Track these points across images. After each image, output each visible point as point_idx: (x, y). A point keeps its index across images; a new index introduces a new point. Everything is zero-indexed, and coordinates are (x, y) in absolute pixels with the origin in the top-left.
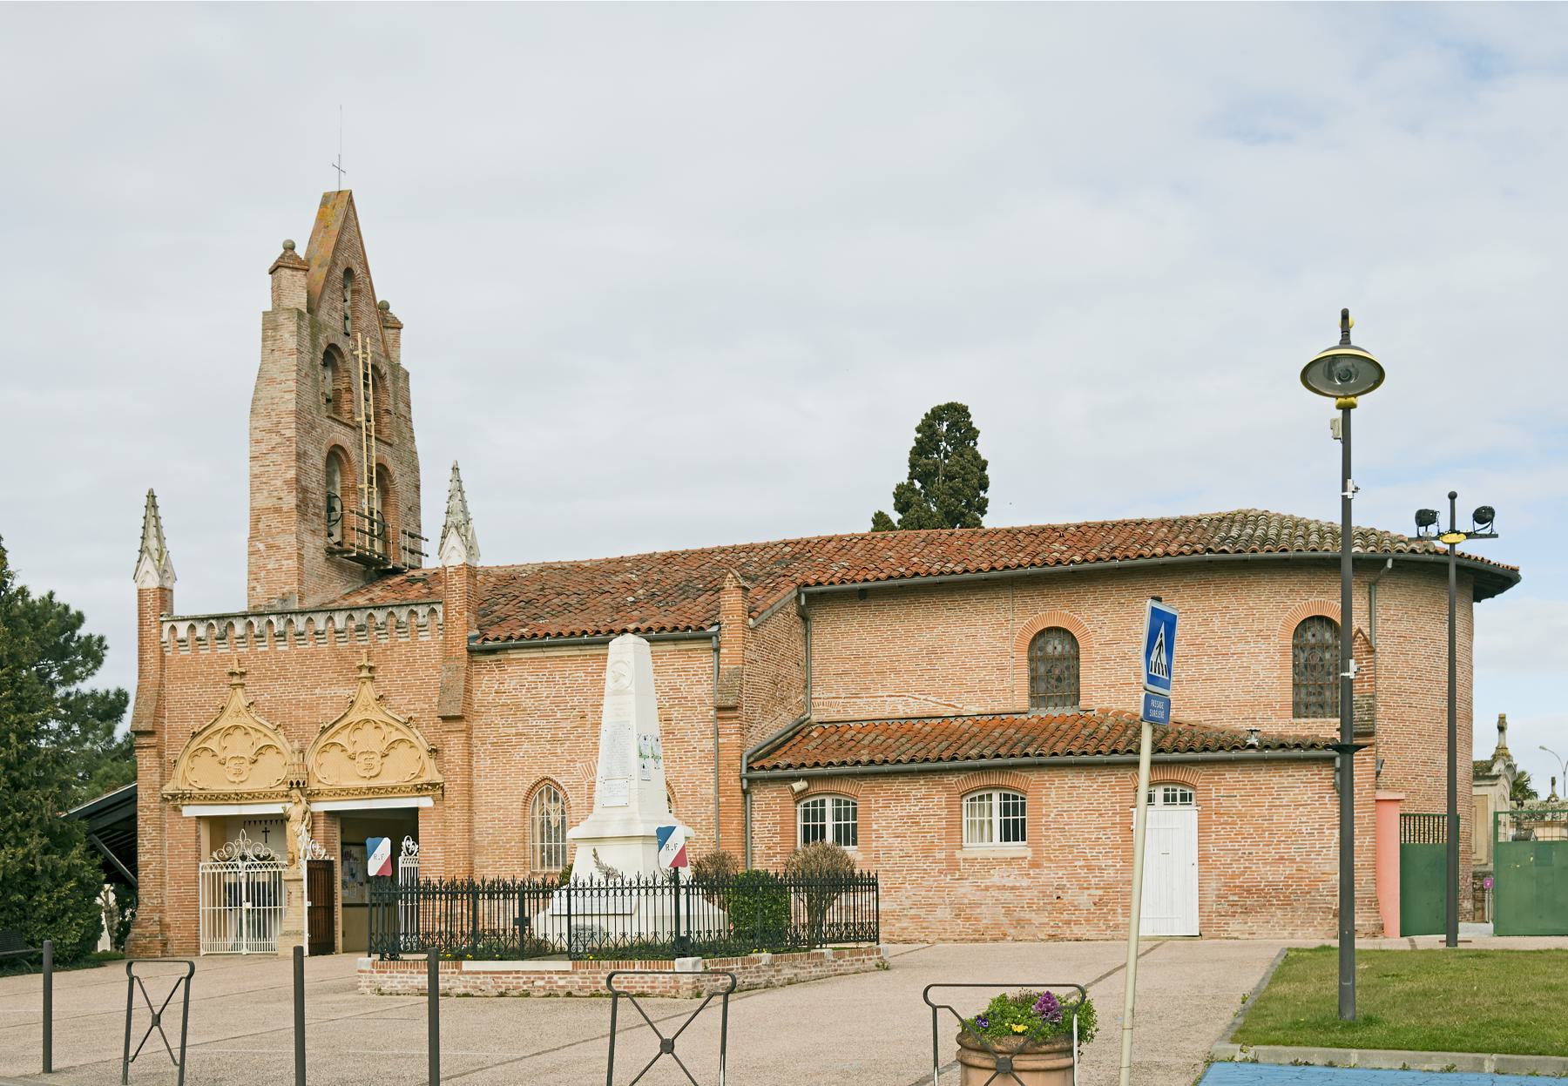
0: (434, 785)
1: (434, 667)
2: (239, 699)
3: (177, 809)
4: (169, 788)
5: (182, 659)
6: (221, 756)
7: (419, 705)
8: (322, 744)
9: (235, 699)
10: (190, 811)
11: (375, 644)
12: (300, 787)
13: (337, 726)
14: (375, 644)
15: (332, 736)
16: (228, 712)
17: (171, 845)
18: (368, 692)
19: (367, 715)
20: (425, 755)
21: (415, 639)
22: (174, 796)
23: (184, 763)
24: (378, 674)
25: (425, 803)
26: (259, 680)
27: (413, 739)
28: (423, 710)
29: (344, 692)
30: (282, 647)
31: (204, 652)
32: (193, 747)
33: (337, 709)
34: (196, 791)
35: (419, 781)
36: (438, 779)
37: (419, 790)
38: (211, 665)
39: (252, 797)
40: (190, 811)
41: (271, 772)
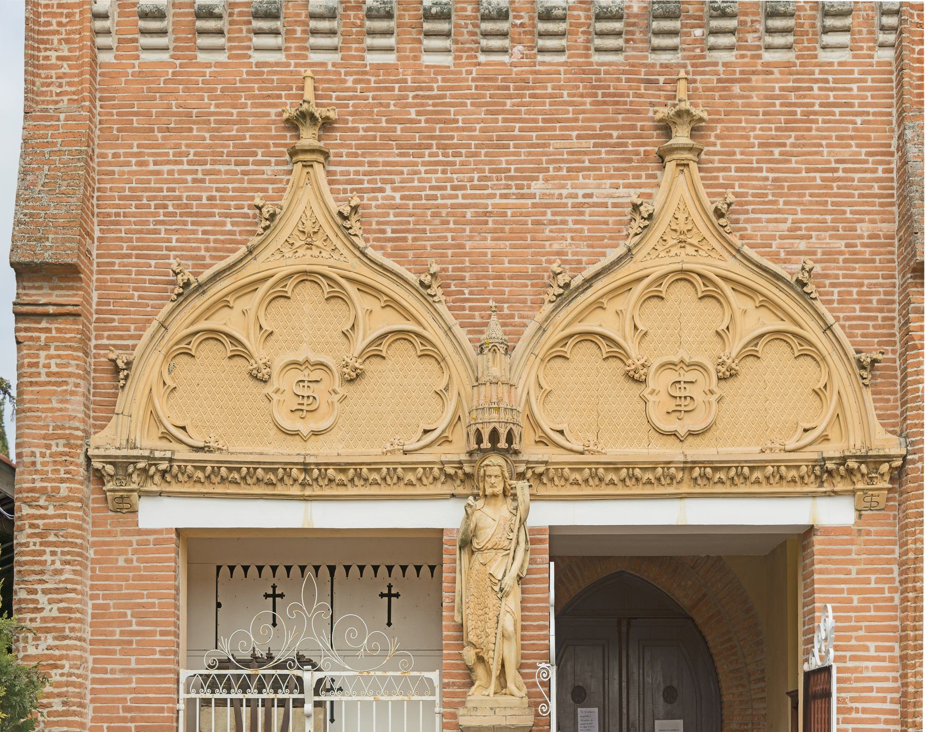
0: (873, 461)
1: (862, 138)
2: (309, 198)
3: (124, 506)
4: (107, 442)
5: (146, 74)
6: (260, 352)
7: (823, 241)
8: (555, 334)
9: (307, 196)
10: (161, 514)
11: (699, 64)
12: (491, 453)
13: (601, 286)
14: (699, 64)
15: (580, 317)
16: (286, 229)
17: (100, 612)
18: (676, 194)
19: (304, 260)
20: (842, 377)
21: (809, 57)
22: (122, 465)
23: (149, 372)
24: (714, 144)
25: (834, 512)
26: (369, 146)
27: (433, 332)
28: (830, 256)
29: (613, 192)
30: (436, 58)
31: (211, 59)
32: (180, 327)
33: (593, 242)
34: (183, 453)
35: (832, 450)
36: (889, 444)
37: (827, 474)
38: (231, 94)
39: (348, 478)
40: (161, 514)
41: (404, 409)
